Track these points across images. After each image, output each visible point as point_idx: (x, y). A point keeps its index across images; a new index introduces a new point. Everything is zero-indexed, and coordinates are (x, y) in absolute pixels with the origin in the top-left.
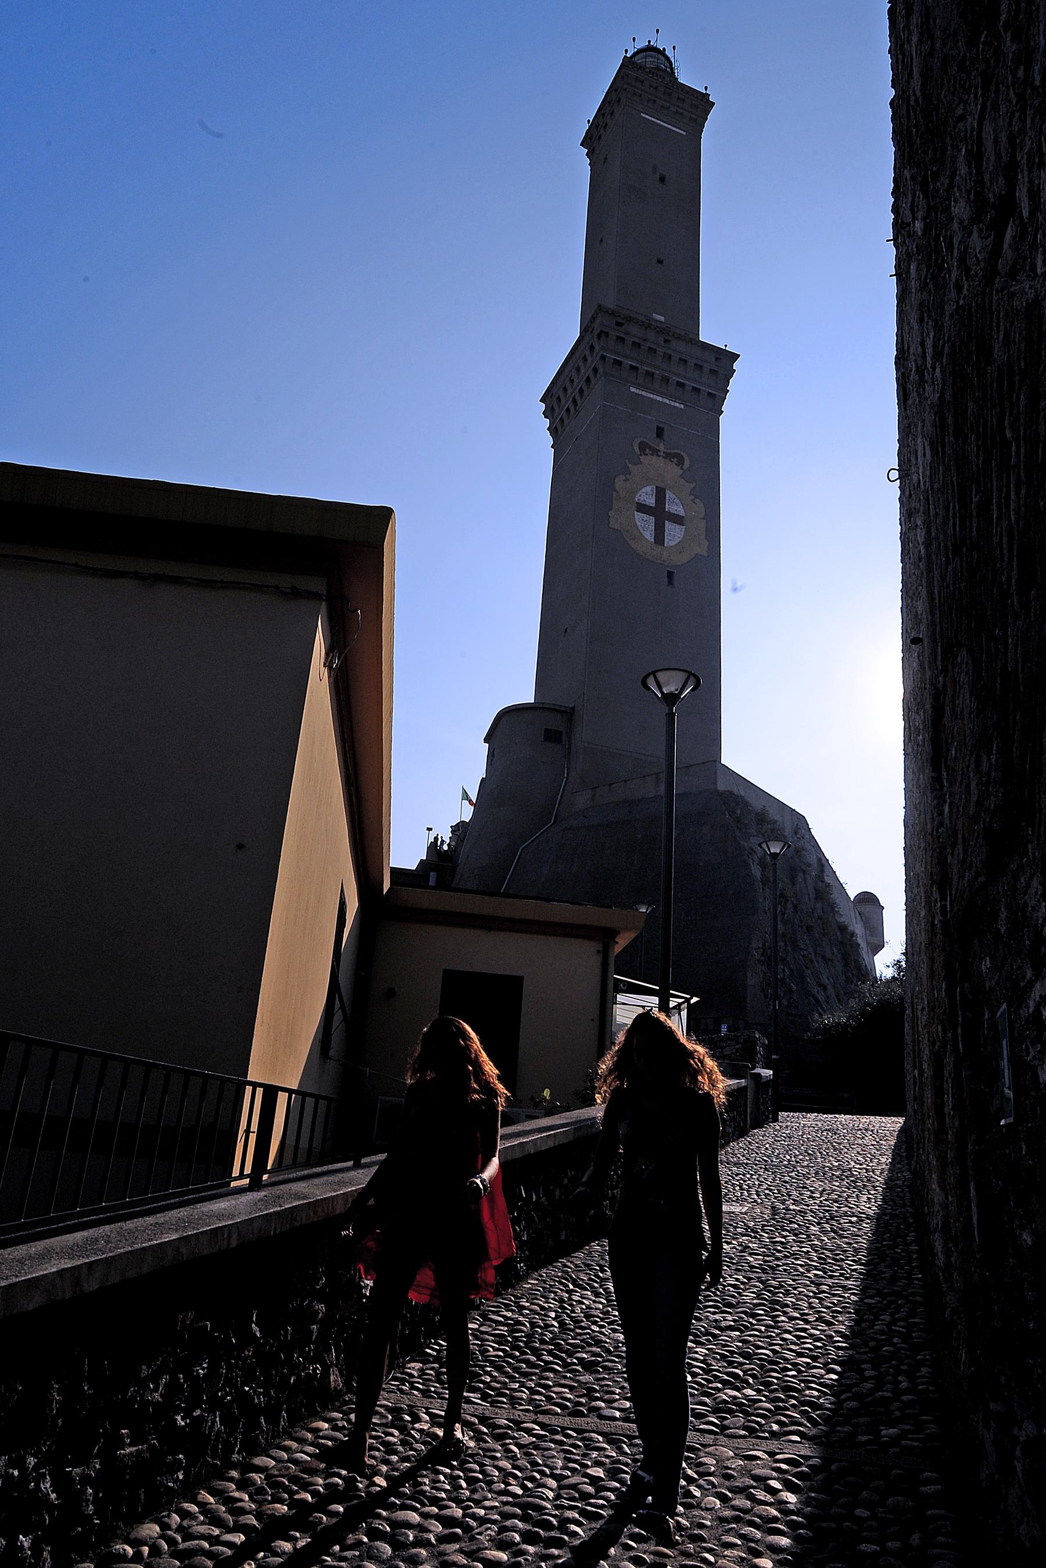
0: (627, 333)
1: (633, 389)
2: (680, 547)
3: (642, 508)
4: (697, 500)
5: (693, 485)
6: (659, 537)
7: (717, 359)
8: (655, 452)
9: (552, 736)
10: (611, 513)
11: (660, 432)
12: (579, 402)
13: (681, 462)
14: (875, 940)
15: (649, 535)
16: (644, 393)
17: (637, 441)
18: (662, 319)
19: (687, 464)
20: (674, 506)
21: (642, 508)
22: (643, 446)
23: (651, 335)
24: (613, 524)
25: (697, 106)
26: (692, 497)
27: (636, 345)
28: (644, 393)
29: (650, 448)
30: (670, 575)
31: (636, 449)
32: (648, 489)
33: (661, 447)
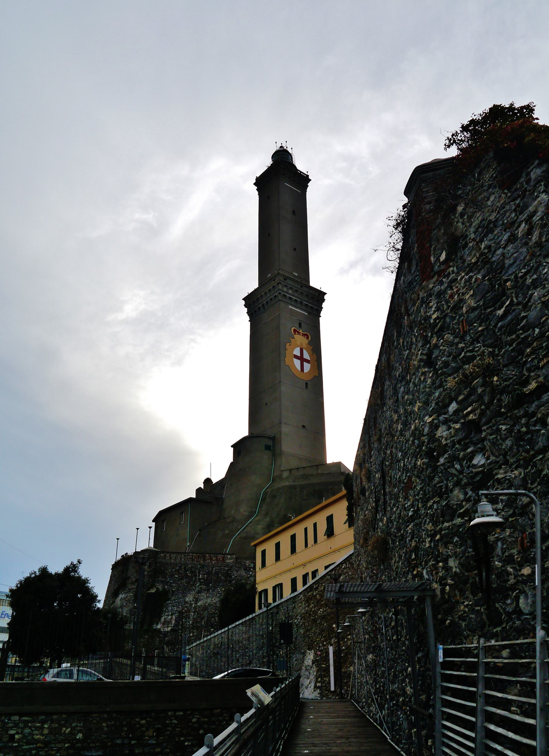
1: (290, 307)
3: (296, 357)
7: (319, 295)
8: (299, 333)
9: (268, 448)
12: (266, 307)
13: (308, 338)
15: (299, 368)
16: (294, 308)
17: (293, 328)
18: (296, 274)
20: (306, 356)
21: (296, 357)
22: (295, 331)
25: (303, 181)
28: (294, 308)
30: (306, 384)
33: (301, 331)
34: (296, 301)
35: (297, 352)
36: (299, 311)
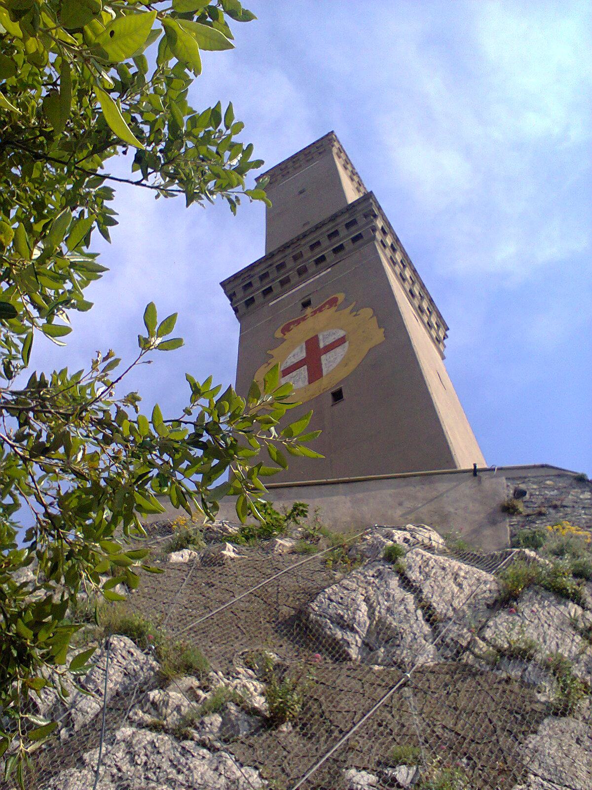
2: (345, 362)
19: (341, 297)
26: (354, 313)
29: (293, 323)
31: (278, 334)
32: (297, 350)
36: (304, 285)
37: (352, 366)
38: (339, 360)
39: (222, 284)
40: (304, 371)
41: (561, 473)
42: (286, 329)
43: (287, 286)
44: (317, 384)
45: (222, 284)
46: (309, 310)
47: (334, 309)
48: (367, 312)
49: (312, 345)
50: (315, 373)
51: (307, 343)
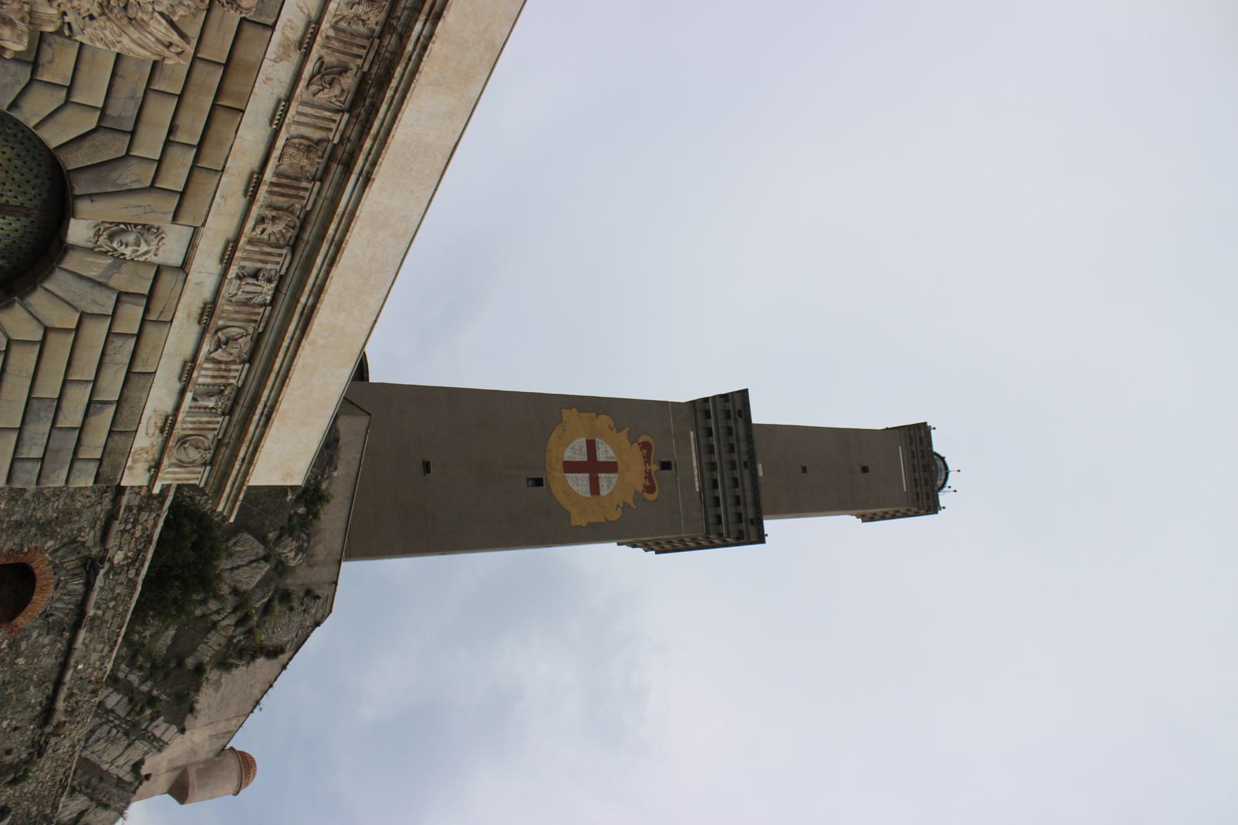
0: (736, 421)
1: (692, 434)
2: (569, 492)
3: (591, 446)
4: (620, 510)
5: (632, 504)
6: (571, 467)
7: (752, 522)
8: (647, 459)
10: (574, 410)
11: (666, 466)
13: (650, 489)
14: (193, 778)
15: (569, 455)
18: (761, 473)
19: (651, 497)
21: (591, 446)
23: (743, 447)
24: (566, 413)
27: (729, 431)
30: (538, 482)
31: (643, 439)
32: (611, 453)
34: (711, 449)
35: (605, 453)
36: (695, 464)
37: (562, 499)
38: (575, 488)
39: (744, 393)
40: (585, 459)
41: (324, 617)
42: (646, 446)
43: (703, 450)
44: (560, 466)
45: (744, 393)
46: (654, 467)
47: (640, 488)
48: (616, 515)
49: (611, 467)
50: (571, 467)
51: (615, 463)
